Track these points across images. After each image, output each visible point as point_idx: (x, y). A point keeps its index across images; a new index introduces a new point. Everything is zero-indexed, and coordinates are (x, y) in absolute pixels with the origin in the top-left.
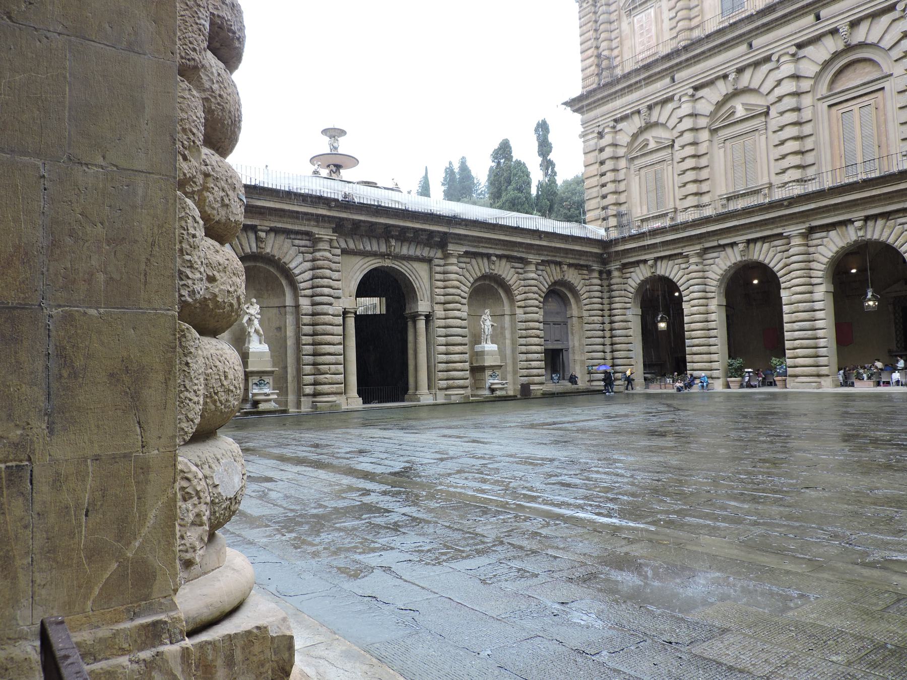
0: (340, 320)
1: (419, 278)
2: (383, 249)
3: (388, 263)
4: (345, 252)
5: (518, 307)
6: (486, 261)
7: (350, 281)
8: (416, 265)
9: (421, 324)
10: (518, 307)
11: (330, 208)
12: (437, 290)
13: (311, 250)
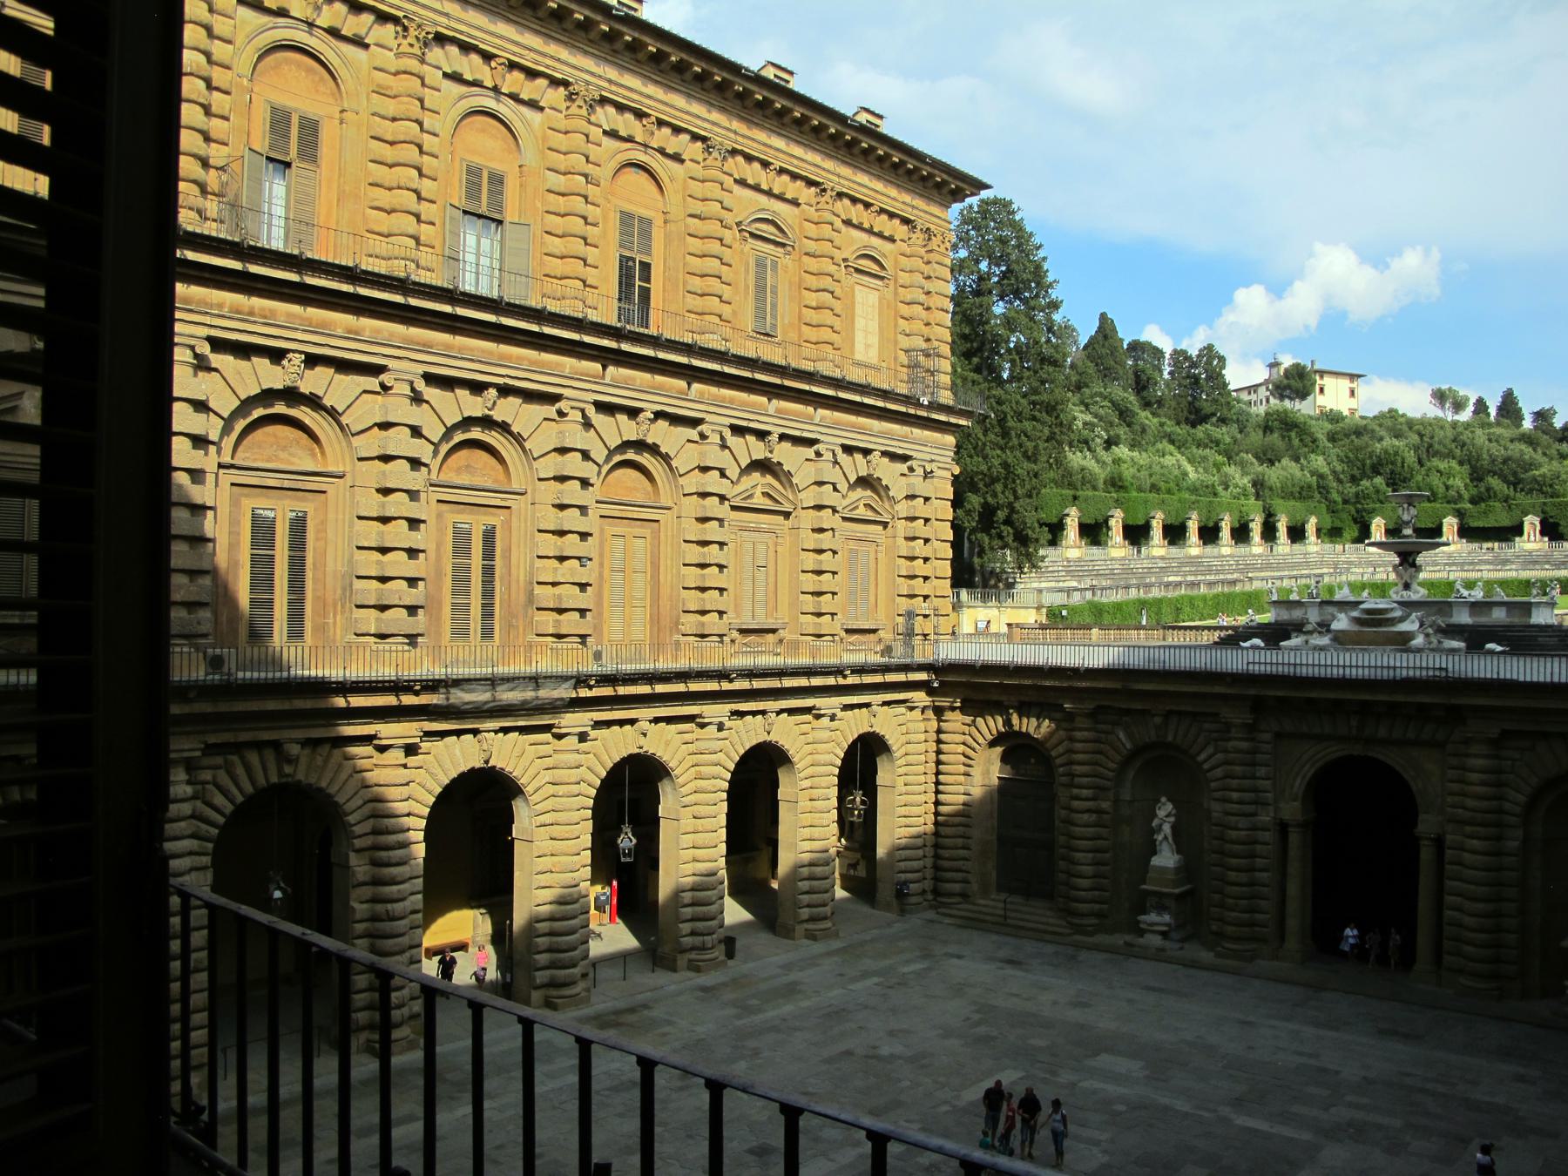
3: (1357, 750)
9: (1426, 854)
12: (1449, 799)
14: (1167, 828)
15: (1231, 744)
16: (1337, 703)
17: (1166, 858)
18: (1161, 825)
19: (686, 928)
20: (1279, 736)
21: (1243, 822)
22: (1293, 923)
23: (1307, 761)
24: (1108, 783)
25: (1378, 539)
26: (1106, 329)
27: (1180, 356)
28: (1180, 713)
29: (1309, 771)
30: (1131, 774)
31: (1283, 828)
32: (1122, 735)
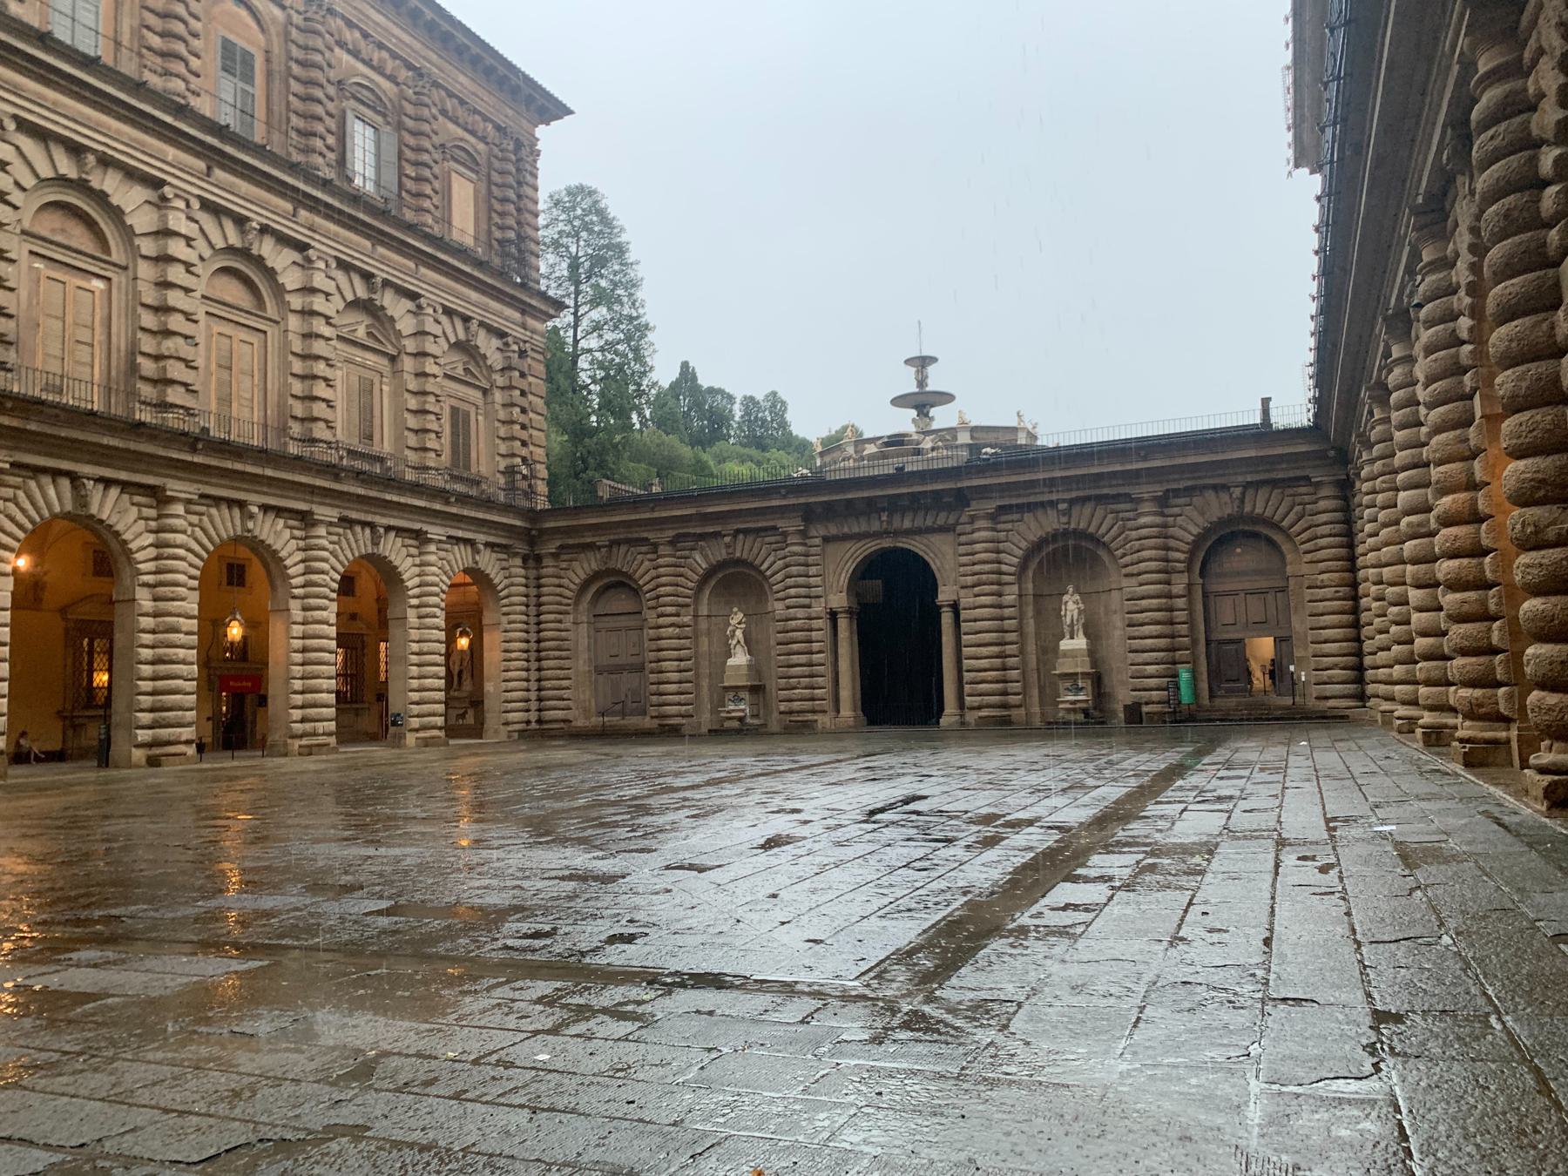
2: (875, 526)
3: (887, 543)
4: (826, 540)
5: (1126, 575)
8: (936, 539)
9: (946, 619)
11: (784, 497)
12: (962, 569)
14: (739, 633)
16: (870, 501)
17: (740, 658)
18: (734, 631)
19: (297, 714)
20: (826, 540)
21: (800, 613)
22: (846, 693)
23: (846, 559)
24: (688, 600)
26: (687, 373)
27: (750, 402)
28: (746, 532)
29: (851, 566)
30: (707, 592)
31: (833, 616)
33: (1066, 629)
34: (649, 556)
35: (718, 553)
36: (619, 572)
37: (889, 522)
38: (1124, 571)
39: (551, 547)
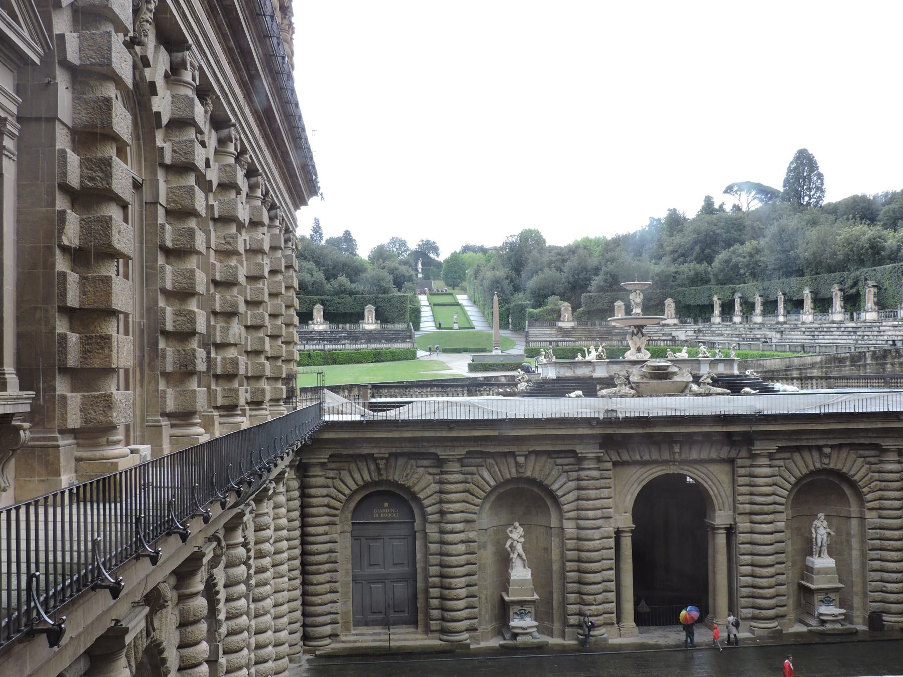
0: (612, 542)
1: (717, 483)
2: (666, 456)
4: (615, 464)
5: (869, 509)
6: (816, 454)
7: (626, 496)
9: (721, 540)
10: (869, 509)
11: (592, 427)
13: (576, 467)
14: (519, 548)
15: (583, 474)
17: (520, 573)
25: (620, 317)
28: (537, 453)
32: (486, 475)
33: (815, 549)
34: (431, 470)
35: (510, 472)
36: (395, 484)
37: (680, 453)
38: (870, 505)
39: (323, 457)
